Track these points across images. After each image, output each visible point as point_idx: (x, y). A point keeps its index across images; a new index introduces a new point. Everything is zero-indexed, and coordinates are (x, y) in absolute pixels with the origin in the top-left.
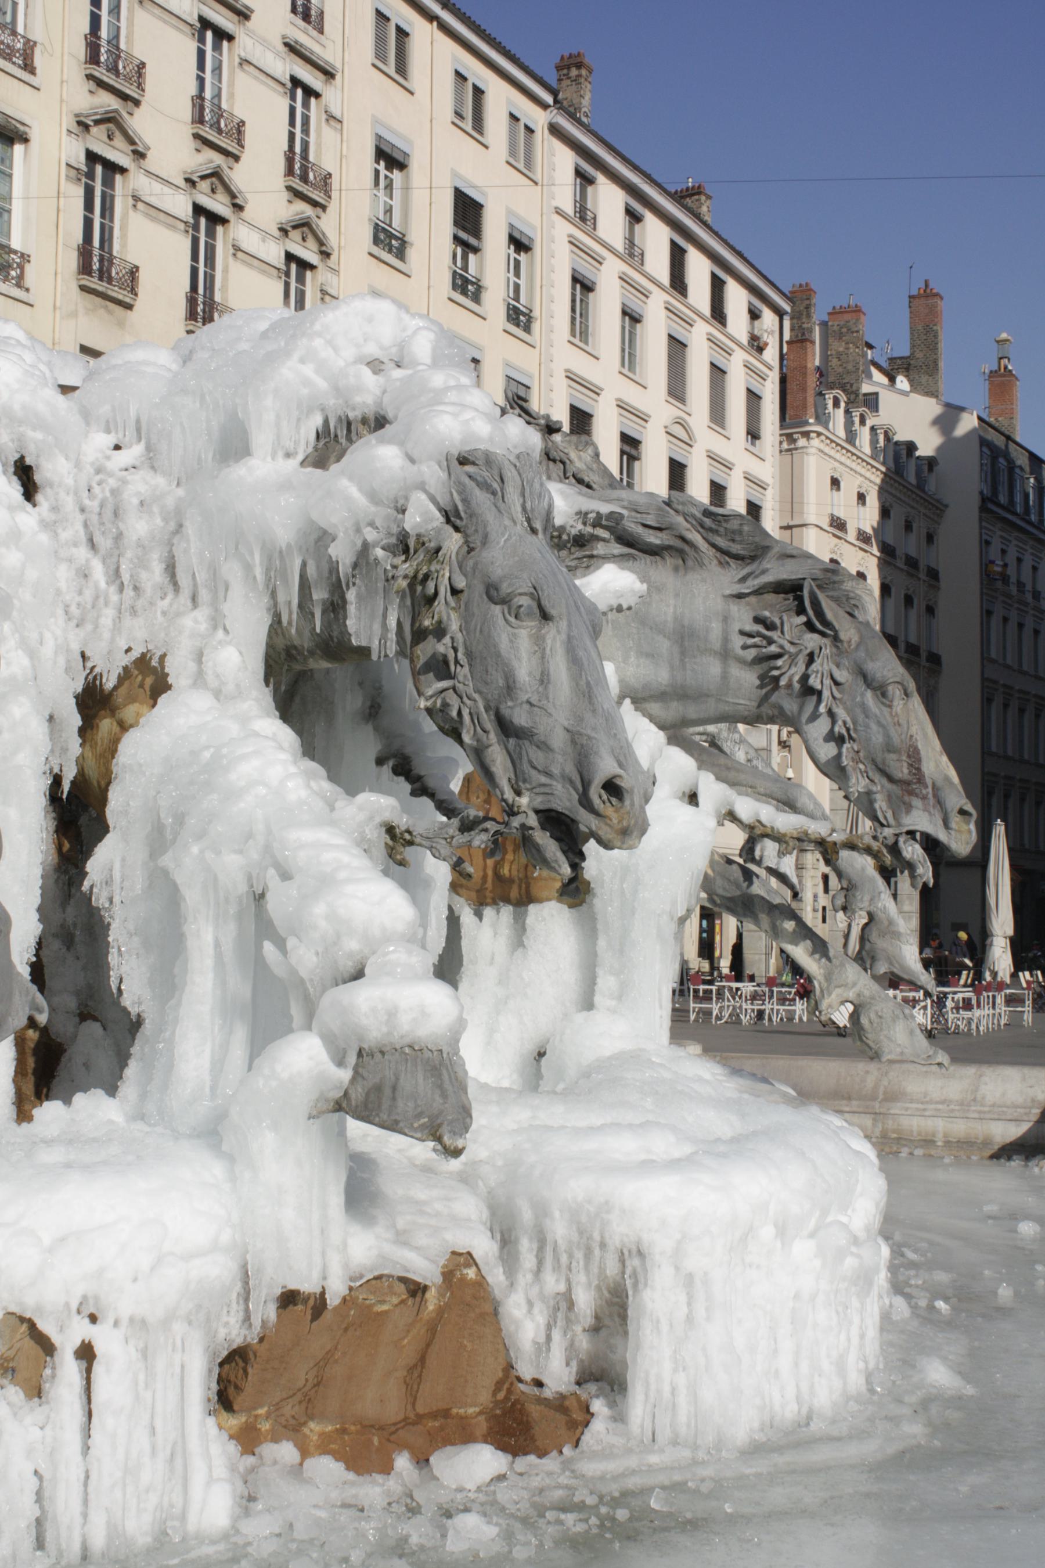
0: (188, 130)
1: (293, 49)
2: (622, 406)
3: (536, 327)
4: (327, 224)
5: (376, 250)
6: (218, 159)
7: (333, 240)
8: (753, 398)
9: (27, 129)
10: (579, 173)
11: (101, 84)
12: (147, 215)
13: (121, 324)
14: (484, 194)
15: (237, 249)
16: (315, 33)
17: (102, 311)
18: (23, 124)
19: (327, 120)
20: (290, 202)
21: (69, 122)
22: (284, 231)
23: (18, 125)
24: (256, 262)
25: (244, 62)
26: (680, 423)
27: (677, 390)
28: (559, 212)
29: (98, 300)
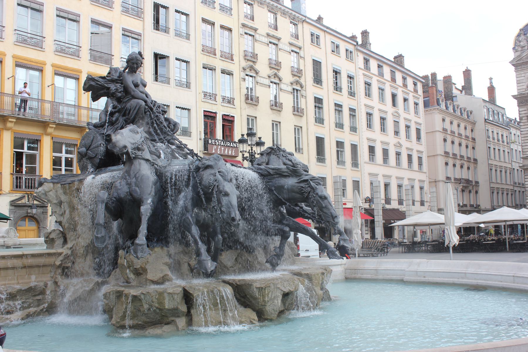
1: (291, 44)
2: (380, 110)
3: (356, 95)
4: (302, 81)
6: (276, 71)
7: (303, 83)
10: (365, 59)
12: (260, 86)
13: (256, 109)
14: (341, 68)
15: (281, 89)
16: (296, 40)
21: (241, 69)
22: (292, 84)
24: (286, 92)
25: (280, 49)
26: (397, 112)
27: (394, 104)
28: (360, 68)
29: (250, 105)
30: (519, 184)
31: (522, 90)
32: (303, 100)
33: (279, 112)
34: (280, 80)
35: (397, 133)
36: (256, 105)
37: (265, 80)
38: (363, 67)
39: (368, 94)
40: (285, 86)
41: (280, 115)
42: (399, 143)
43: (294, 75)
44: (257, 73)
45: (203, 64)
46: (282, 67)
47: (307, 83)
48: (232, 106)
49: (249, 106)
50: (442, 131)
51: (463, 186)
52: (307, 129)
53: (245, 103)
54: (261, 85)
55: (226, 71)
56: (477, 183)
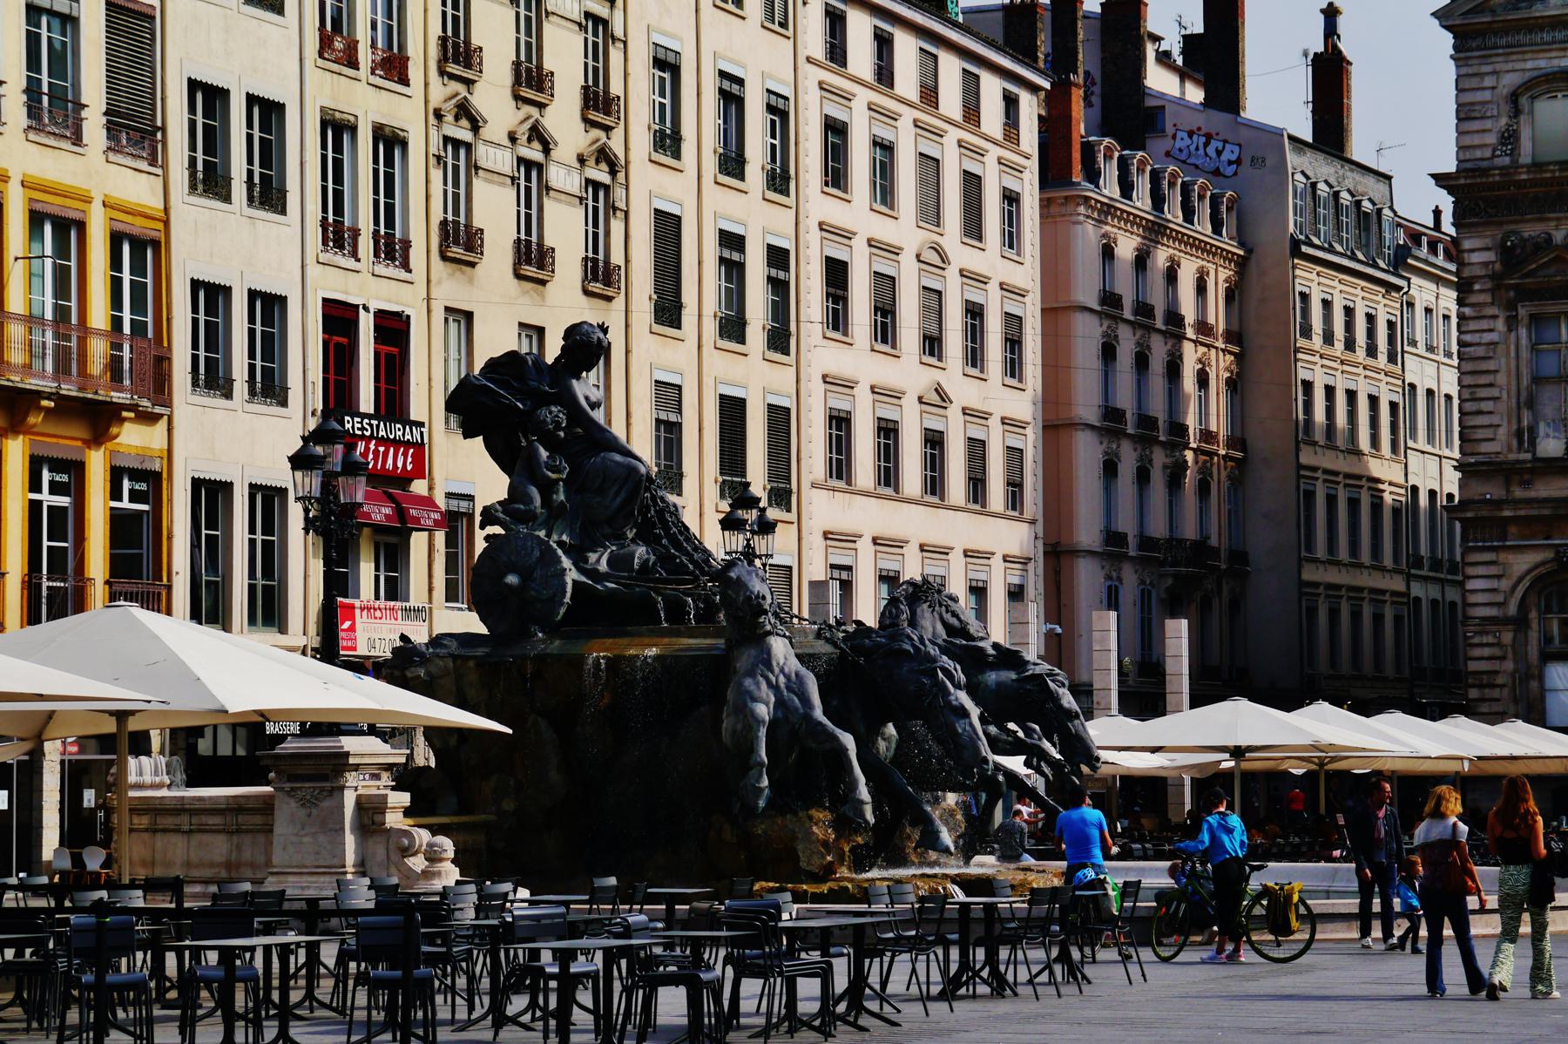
0: (508, 93)
4: (616, 144)
5: (656, 157)
6: (534, 111)
8: (1011, 199)
9: (405, 134)
11: (452, 77)
12: (486, 180)
13: (471, 281)
14: (744, 67)
17: (458, 274)
18: (403, 130)
19: (613, 43)
20: (586, 131)
23: (400, 133)
28: (809, 60)
30: (1436, 564)
31: (1478, 154)
32: (617, 226)
33: (540, 287)
34: (547, 150)
35: (933, 344)
36: (472, 265)
37: (499, 152)
38: (819, 52)
39: (836, 177)
40: (562, 171)
41: (542, 296)
42: (939, 391)
43: (590, 123)
44: (475, 128)
45: (323, 109)
46: (556, 91)
47: (633, 156)
48: (403, 275)
49: (451, 266)
50: (1098, 308)
51: (1176, 576)
52: (627, 352)
53: (438, 258)
54: (489, 176)
55: (387, 130)
56: (1239, 557)
